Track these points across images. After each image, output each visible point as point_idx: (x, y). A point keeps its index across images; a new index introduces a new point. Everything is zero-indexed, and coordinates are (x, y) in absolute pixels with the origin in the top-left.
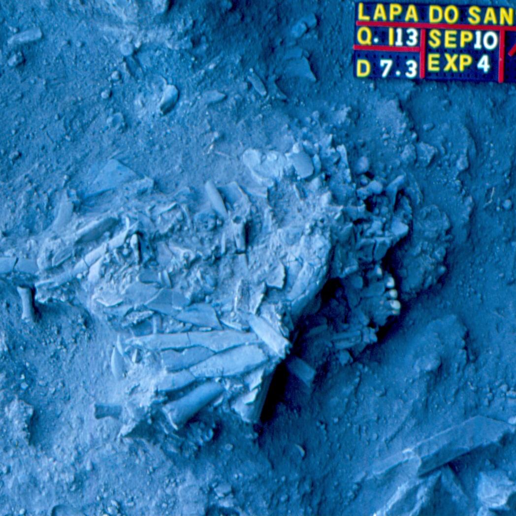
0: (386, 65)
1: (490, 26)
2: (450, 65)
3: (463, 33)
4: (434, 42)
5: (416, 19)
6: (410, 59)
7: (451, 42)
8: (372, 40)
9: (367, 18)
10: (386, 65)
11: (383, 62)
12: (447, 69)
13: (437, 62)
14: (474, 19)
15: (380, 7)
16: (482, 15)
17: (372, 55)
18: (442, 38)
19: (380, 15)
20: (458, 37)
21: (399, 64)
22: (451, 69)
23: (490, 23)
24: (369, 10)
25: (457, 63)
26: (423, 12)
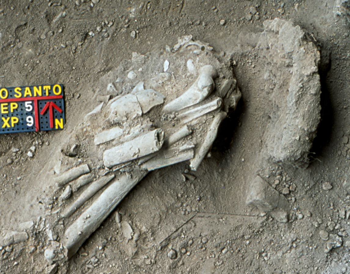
1: (28, 98)
3: (12, 104)
7: (4, 110)
12: (4, 126)
14: (18, 95)
16: (22, 92)
20: (8, 106)
22: (6, 127)
23: (28, 96)
25: (9, 122)
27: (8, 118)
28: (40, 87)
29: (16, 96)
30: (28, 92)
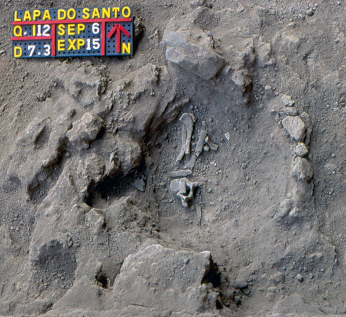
0: (31, 49)
2: (72, 46)
3: (79, 25)
4: (61, 32)
5: (50, 19)
6: (47, 44)
7: (71, 32)
8: (23, 33)
9: (19, 20)
10: (31, 49)
11: (29, 47)
12: (69, 49)
13: (63, 45)
14: (86, 16)
15: (27, 12)
16: (90, 13)
17: (23, 42)
18: (66, 29)
19: (27, 17)
21: (40, 48)
22: (72, 49)
23: (96, 17)
24: (21, 14)
25: (75, 44)
26: (54, 14)
27: (75, 40)
28: (109, 9)
29: (83, 16)
30: (96, 13)
